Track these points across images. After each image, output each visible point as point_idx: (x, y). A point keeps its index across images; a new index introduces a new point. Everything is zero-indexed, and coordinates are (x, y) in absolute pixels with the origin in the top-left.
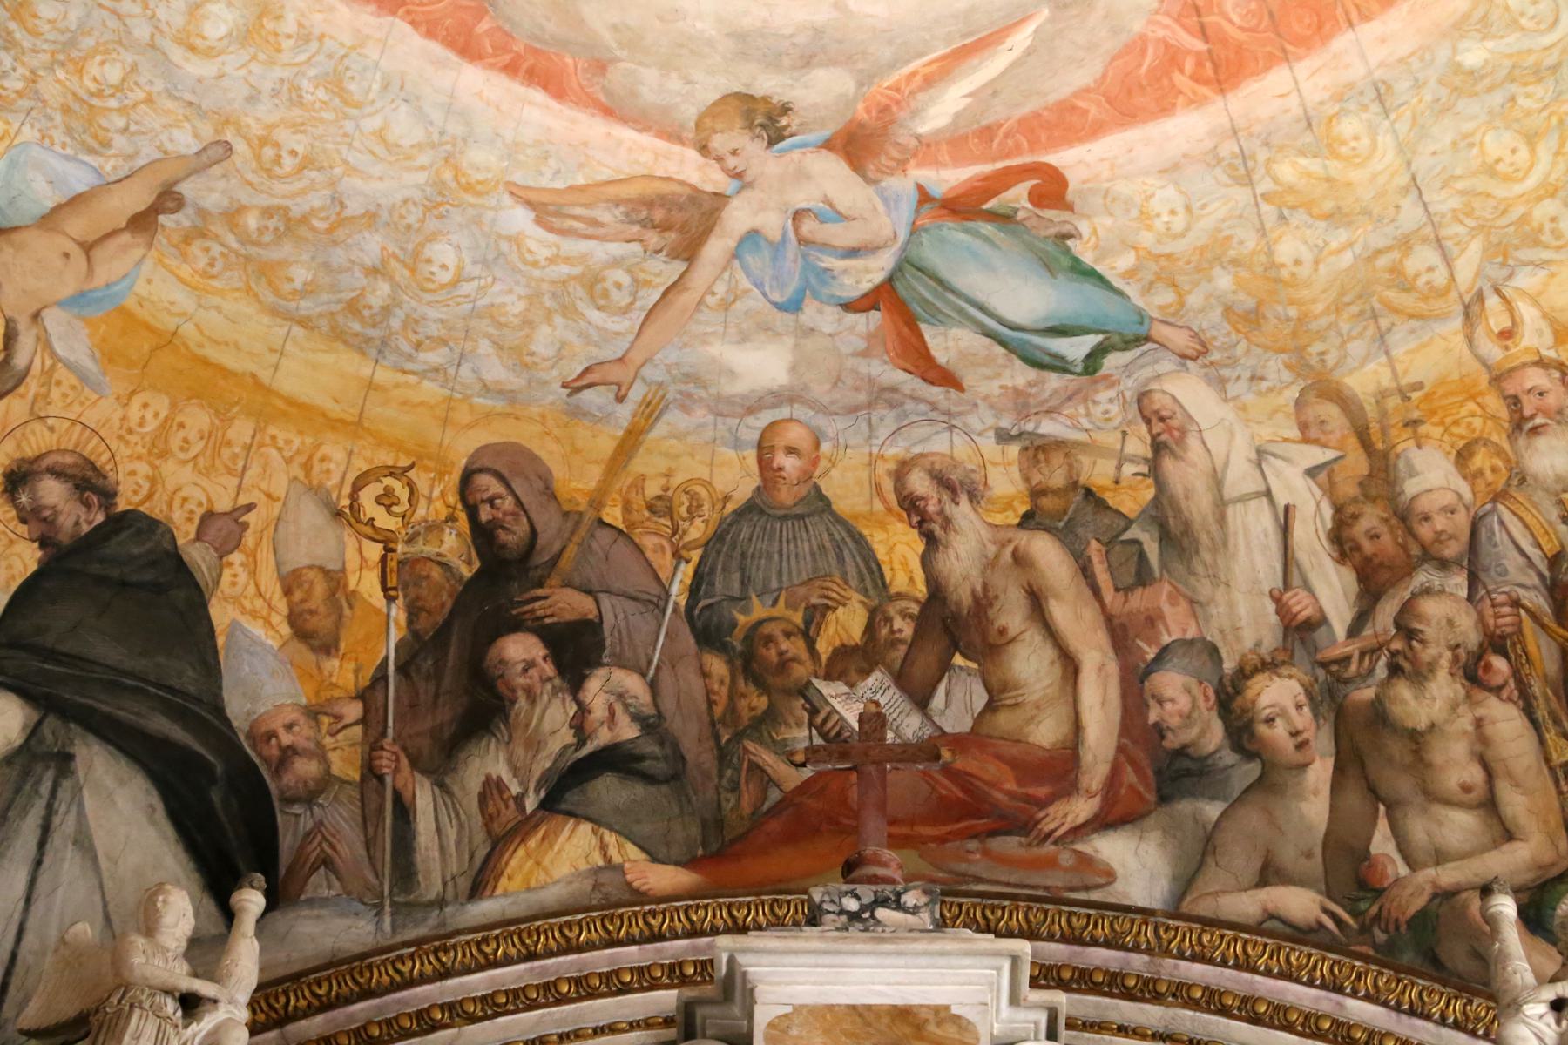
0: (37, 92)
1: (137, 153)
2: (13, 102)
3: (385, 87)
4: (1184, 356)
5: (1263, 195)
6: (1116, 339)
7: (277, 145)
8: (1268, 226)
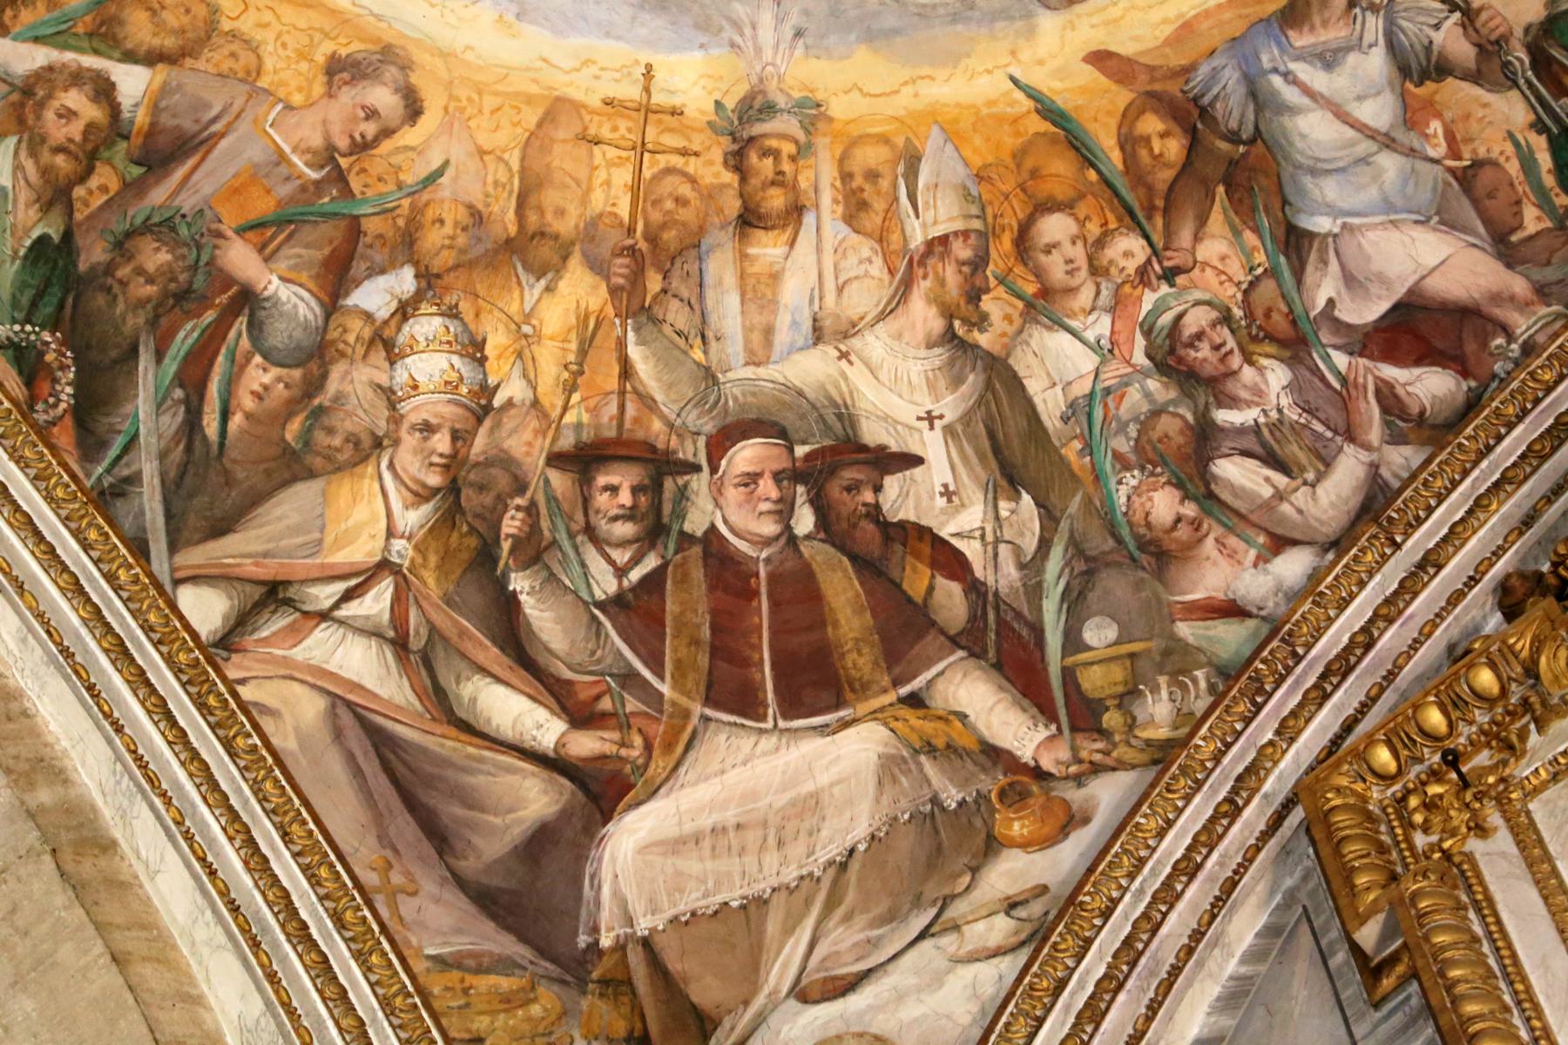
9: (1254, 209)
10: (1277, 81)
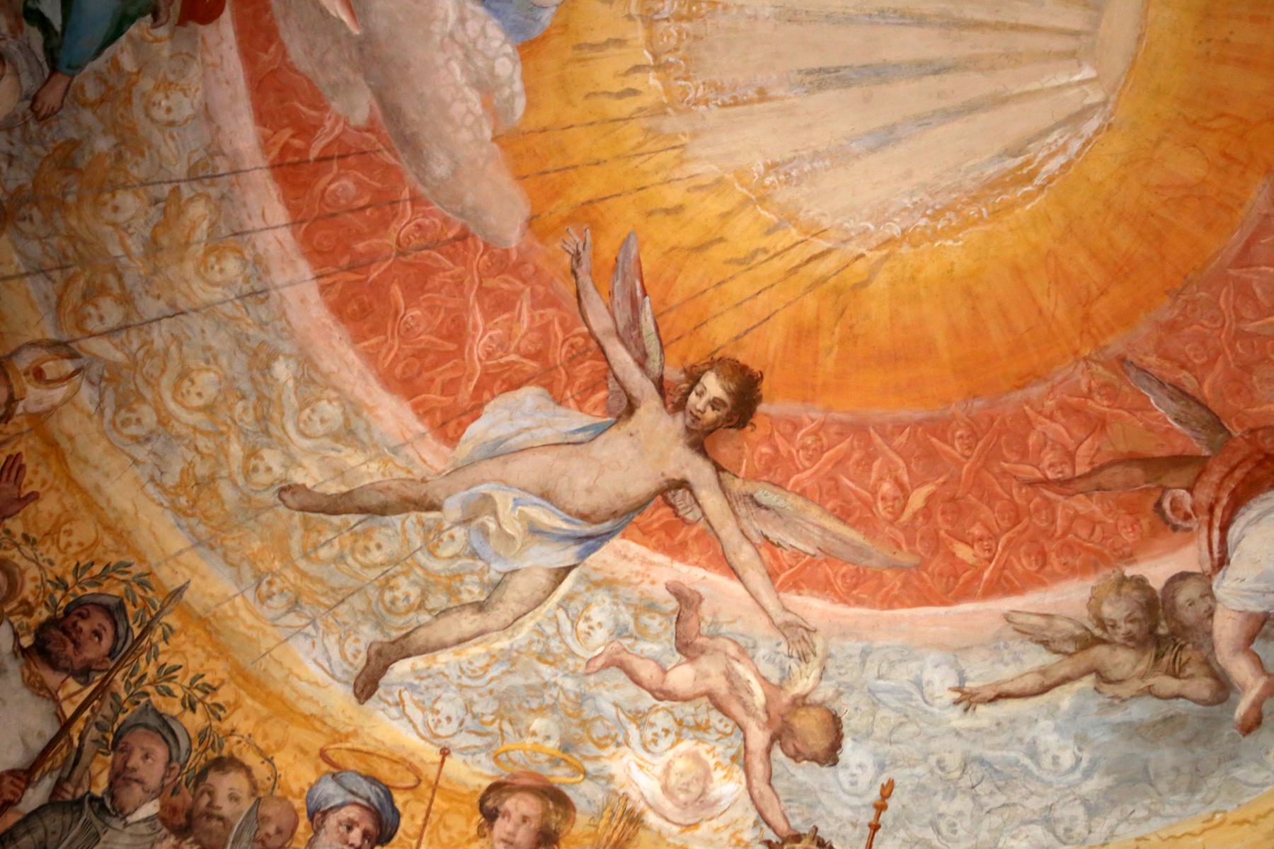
4: (35, 99)
5: (178, 188)
6: (55, 42)
8: (150, 188)
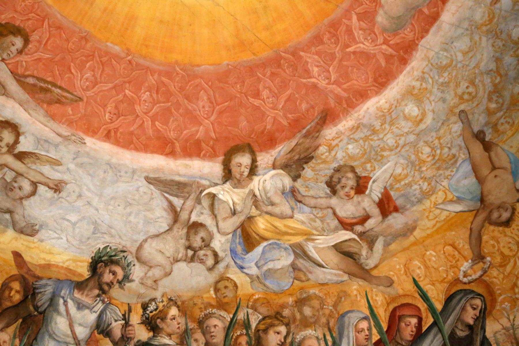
0: (430, 178)
1: (459, 145)
2: (432, 187)
3: (446, 50)
7: (463, 93)
9: (25, 334)
10: (61, 301)
